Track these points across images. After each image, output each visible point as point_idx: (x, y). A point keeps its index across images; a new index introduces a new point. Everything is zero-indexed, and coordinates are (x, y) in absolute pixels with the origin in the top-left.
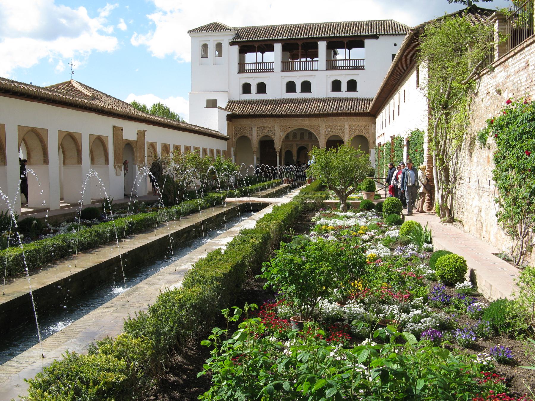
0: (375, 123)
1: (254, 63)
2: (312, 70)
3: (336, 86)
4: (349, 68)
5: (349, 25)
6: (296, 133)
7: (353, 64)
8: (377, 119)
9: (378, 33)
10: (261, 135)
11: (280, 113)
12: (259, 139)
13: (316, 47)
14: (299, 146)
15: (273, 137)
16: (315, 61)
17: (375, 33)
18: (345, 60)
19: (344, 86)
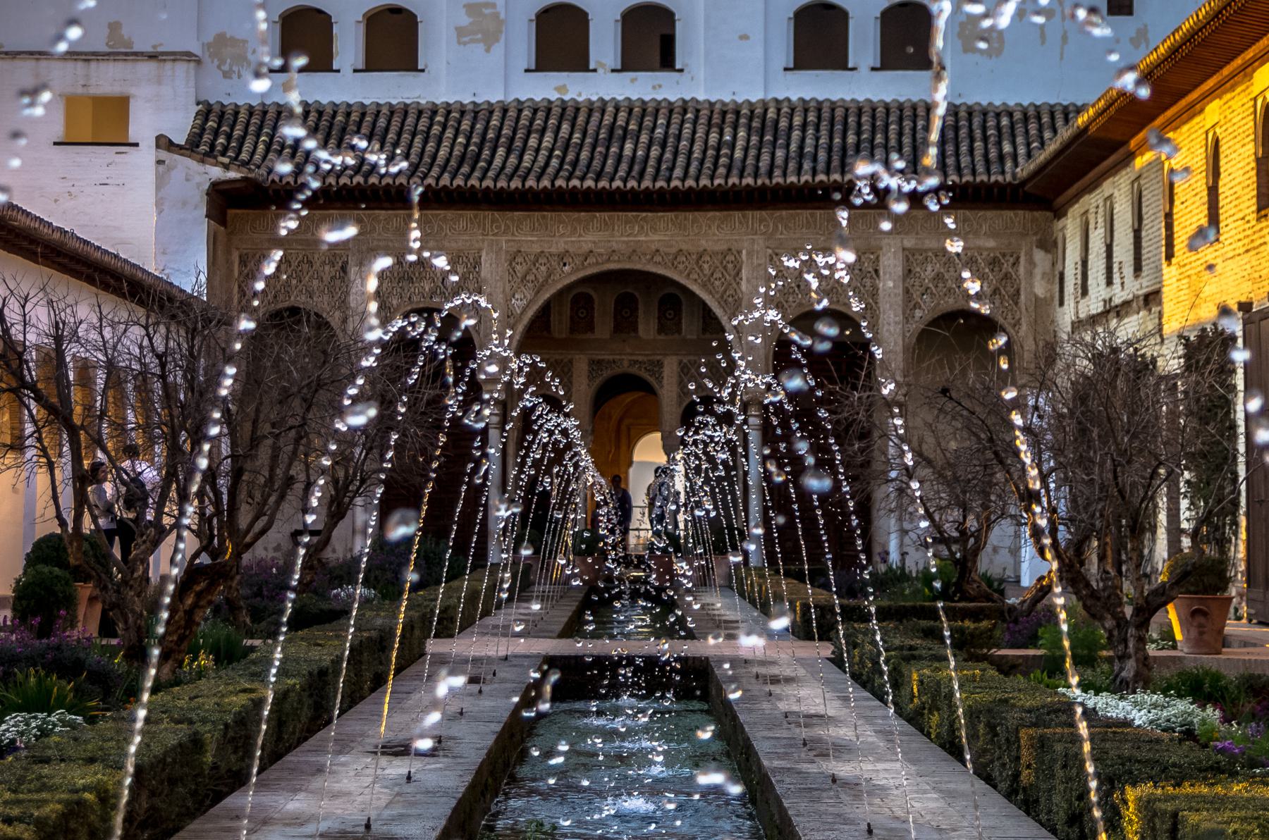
0: (1051, 245)
6: (589, 299)
8: (1070, 226)
11: (516, 183)
14: (607, 374)
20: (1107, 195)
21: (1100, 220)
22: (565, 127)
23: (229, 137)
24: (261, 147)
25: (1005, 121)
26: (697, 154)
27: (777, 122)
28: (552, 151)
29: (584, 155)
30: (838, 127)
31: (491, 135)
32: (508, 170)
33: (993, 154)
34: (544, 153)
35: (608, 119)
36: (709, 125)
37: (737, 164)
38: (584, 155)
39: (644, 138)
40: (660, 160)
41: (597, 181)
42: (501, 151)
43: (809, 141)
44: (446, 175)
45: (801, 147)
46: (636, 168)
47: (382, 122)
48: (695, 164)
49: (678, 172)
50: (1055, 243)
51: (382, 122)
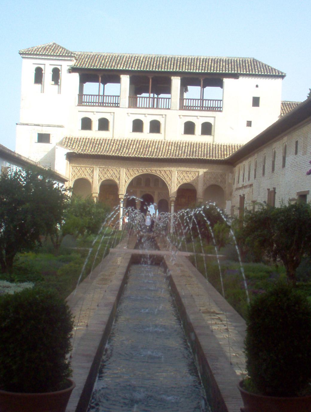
0: (232, 172)
1: (96, 96)
2: (157, 108)
3: (189, 128)
4: (202, 108)
5: (206, 60)
7: (206, 104)
8: (236, 169)
9: (239, 72)
10: (103, 179)
11: (127, 155)
12: (100, 183)
13: (169, 82)
15: (117, 182)
16: (162, 98)
17: (236, 72)
18: (200, 99)
19: (198, 129)
20: (244, 164)
21: (242, 169)
22: (138, 144)
23: (71, 143)
24: (77, 146)
25: (225, 147)
26: (164, 151)
27: (180, 145)
28: (135, 149)
29: (142, 150)
30: (192, 147)
31: (123, 145)
32: (126, 152)
33: (223, 154)
34: (133, 149)
35: (146, 143)
36: (166, 145)
37: (172, 154)
38: (142, 150)
39: (153, 147)
40: (156, 152)
41: (143, 156)
42: (125, 149)
43: (186, 150)
44: (114, 153)
45: (185, 150)
46: (152, 154)
47: (101, 142)
48: (163, 153)
49: (160, 155)
50: (233, 172)
51: (101, 142)
